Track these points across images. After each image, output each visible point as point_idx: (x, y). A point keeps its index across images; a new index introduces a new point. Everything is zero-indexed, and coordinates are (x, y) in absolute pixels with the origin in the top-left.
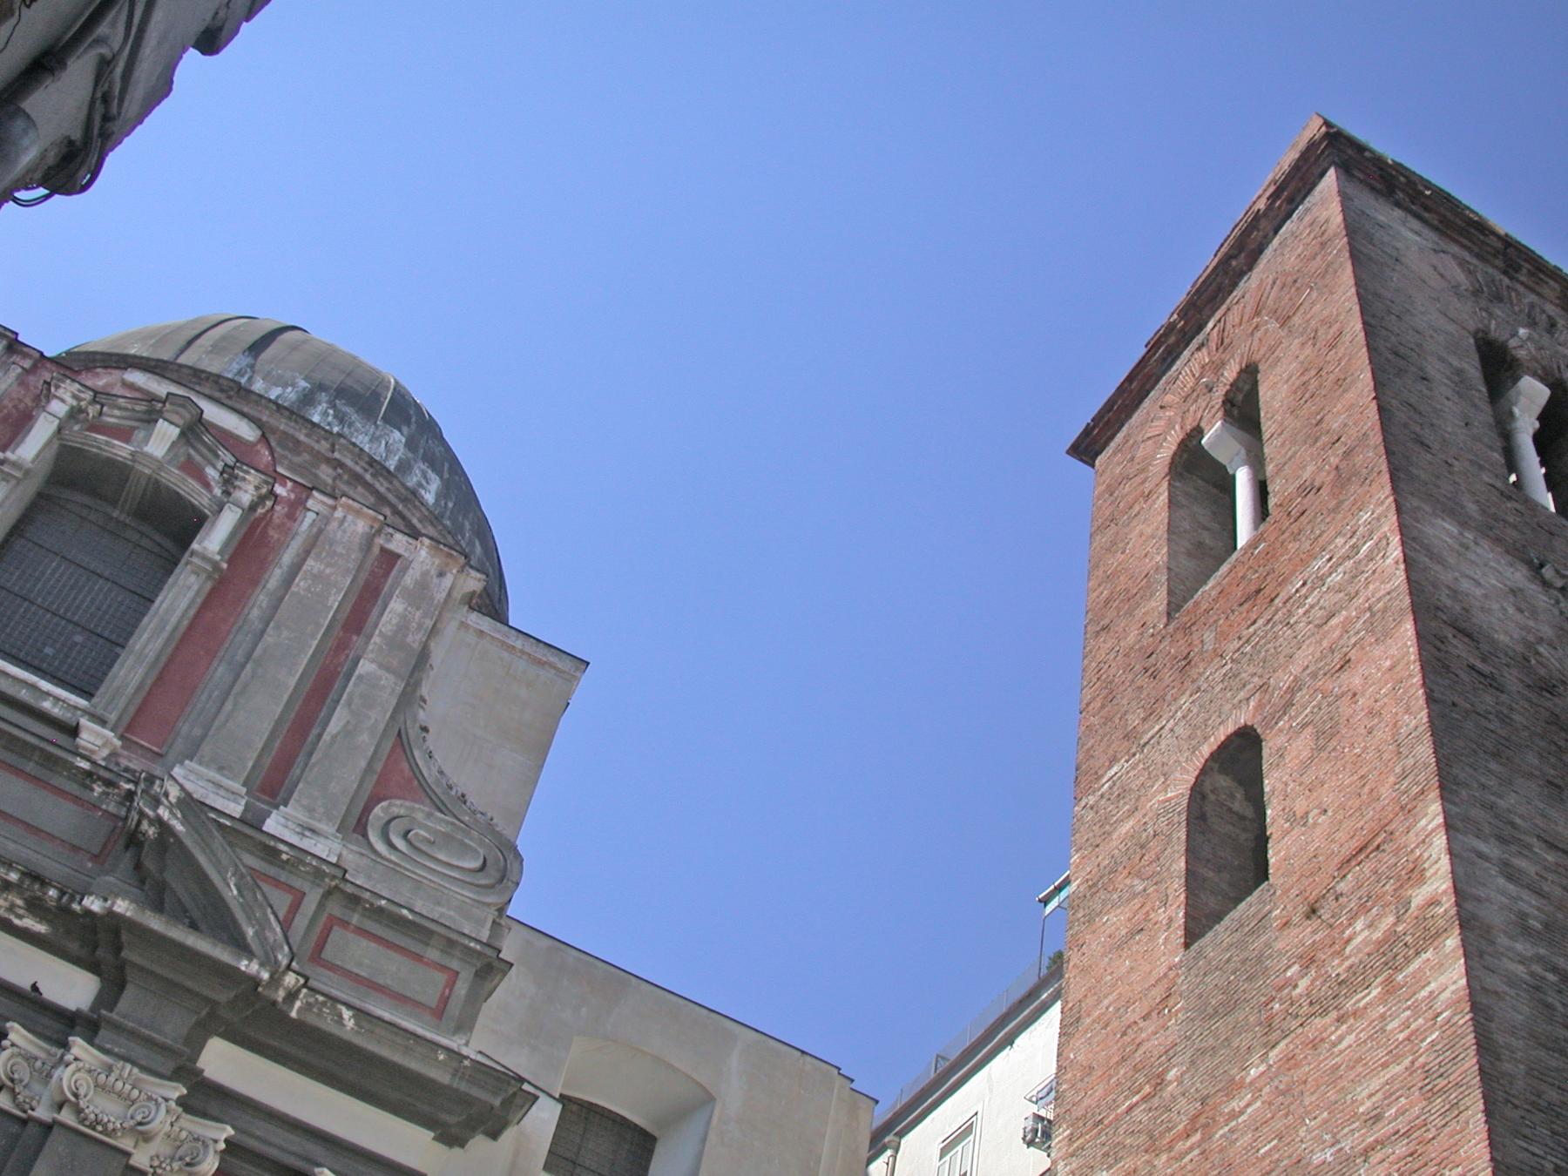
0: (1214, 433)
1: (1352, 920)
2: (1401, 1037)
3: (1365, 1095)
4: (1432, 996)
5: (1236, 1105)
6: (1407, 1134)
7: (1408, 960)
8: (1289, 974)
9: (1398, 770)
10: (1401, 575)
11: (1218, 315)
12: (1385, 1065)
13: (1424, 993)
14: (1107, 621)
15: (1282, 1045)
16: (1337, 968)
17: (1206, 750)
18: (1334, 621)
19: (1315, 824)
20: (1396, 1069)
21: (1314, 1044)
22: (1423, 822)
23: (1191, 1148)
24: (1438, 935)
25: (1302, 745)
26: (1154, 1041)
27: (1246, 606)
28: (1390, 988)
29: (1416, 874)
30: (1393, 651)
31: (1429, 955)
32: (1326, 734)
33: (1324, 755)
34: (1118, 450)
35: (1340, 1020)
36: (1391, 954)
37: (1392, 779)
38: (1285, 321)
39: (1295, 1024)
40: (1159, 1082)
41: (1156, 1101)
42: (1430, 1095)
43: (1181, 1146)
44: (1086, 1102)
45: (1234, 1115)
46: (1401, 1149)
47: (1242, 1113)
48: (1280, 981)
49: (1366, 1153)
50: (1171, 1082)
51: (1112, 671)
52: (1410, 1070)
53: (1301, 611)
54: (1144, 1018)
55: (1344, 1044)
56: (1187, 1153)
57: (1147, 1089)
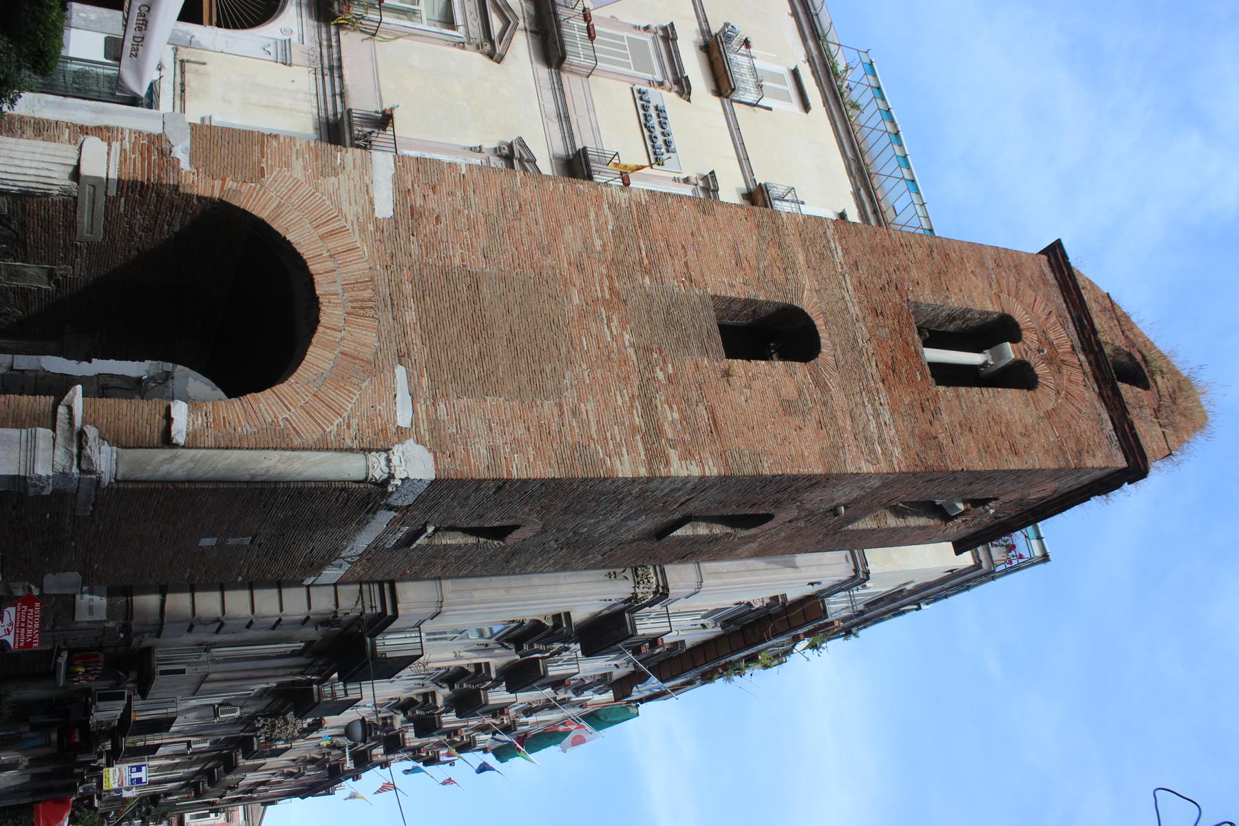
0: (1010, 351)
1: (681, 411)
2: (608, 434)
3: (589, 408)
4: (620, 455)
5: (615, 324)
6: (560, 432)
7: (645, 443)
8: (670, 366)
9: (746, 452)
10: (851, 469)
11: (1086, 365)
12: (598, 422)
13: (625, 452)
14: (935, 254)
15: (634, 358)
16: (660, 398)
17: (819, 323)
18: (848, 422)
20: (594, 427)
21: (626, 379)
22: (711, 463)
23: (602, 291)
24: (650, 464)
25: (790, 391)
26: (671, 271)
27: (890, 362)
28: (634, 430)
29: (687, 455)
30: (812, 459)
31: (643, 457)
32: (788, 407)
33: (777, 404)
34: (1042, 274)
36: (653, 431)
37: (743, 447)
38: (1048, 415)
39: (642, 366)
40: (647, 272)
41: (637, 268)
42: (573, 448)
43: (606, 283)
44: (655, 216)
45: (609, 320)
46: (554, 427)
47: (609, 326)
48: (669, 360)
49: (561, 405)
50: (643, 278)
51: (901, 256)
52: (591, 438)
53: (866, 400)
54: (686, 263)
55: (619, 397)
56: (601, 287)
57: (646, 262)
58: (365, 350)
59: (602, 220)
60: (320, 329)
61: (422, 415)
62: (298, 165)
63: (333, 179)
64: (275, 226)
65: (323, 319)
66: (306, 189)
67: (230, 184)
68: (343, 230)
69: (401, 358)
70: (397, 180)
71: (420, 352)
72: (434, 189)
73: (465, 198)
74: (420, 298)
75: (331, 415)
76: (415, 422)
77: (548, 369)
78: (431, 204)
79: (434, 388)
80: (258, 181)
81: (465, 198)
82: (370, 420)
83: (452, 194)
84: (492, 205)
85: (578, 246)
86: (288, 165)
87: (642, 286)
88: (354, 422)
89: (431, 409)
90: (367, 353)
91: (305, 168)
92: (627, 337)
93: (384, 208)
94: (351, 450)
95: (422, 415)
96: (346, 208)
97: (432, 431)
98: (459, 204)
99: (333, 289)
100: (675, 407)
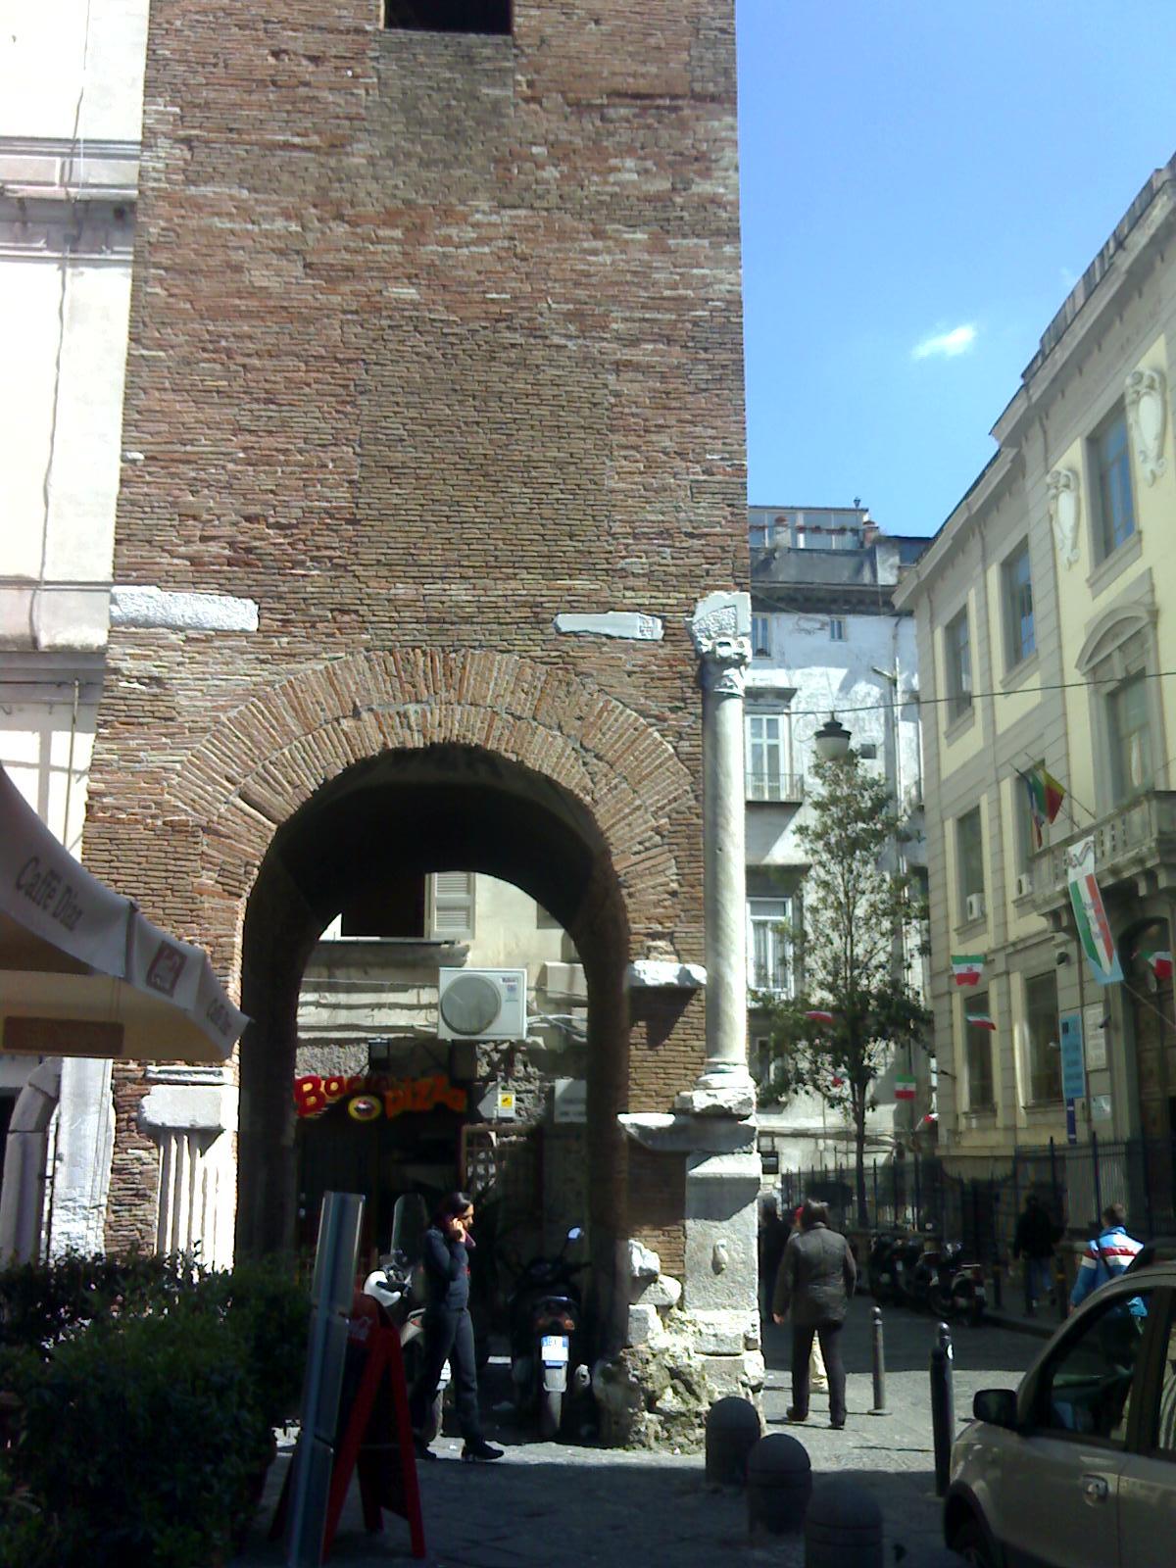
2: (667, 293)
8: (535, 150)
35: (597, 234)
45: (447, 241)
57: (315, 140)
62: (154, 759)
65: (475, 739)
69: (538, 617)
70: (167, 581)
71: (527, 585)
84: (211, 413)
89: (631, 582)
93: (241, 614)
100: (613, 162)
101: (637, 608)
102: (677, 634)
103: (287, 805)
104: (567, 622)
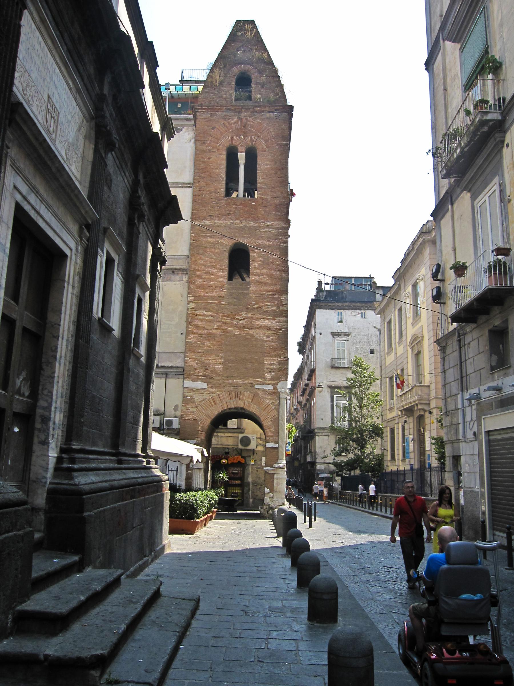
19: (261, 279)
21: (258, 318)
35: (264, 318)
40: (220, 302)
45: (238, 319)
47: (240, 320)
58: (251, 396)
59: (202, 314)
60: (245, 407)
61: (270, 382)
62: (191, 410)
63: (195, 399)
64: (213, 417)
65: (242, 406)
66: (199, 407)
67: (200, 429)
68: (213, 398)
69: (253, 386)
71: (251, 380)
72: (196, 369)
73: (198, 359)
74: (234, 378)
75: (269, 407)
76: (271, 384)
77: (254, 343)
78: (202, 370)
79: (261, 378)
80: (198, 421)
81: (198, 359)
82: (271, 397)
83: (197, 363)
85: (212, 325)
86: (191, 412)
87: (225, 305)
88: (271, 401)
90: (252, 396)
91: (192, 408)
92: (243, 315)
93: (205, 385)
94: (279, 402)
95: (270, 382)
96: (205, 397)
97: (274, 380)
98: (200, 362)
99: (232, 402)
101: (269, 384)
102: (275, 388)
103: (213, 417)
104: (257, 387)
